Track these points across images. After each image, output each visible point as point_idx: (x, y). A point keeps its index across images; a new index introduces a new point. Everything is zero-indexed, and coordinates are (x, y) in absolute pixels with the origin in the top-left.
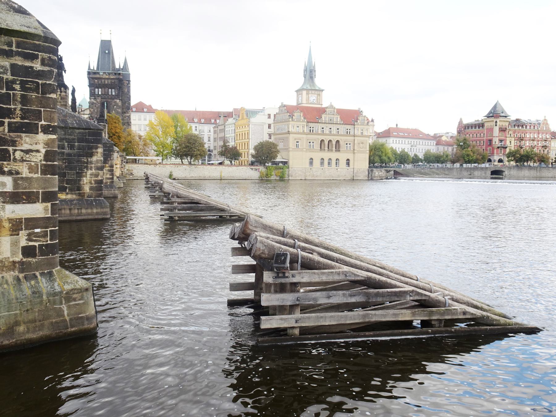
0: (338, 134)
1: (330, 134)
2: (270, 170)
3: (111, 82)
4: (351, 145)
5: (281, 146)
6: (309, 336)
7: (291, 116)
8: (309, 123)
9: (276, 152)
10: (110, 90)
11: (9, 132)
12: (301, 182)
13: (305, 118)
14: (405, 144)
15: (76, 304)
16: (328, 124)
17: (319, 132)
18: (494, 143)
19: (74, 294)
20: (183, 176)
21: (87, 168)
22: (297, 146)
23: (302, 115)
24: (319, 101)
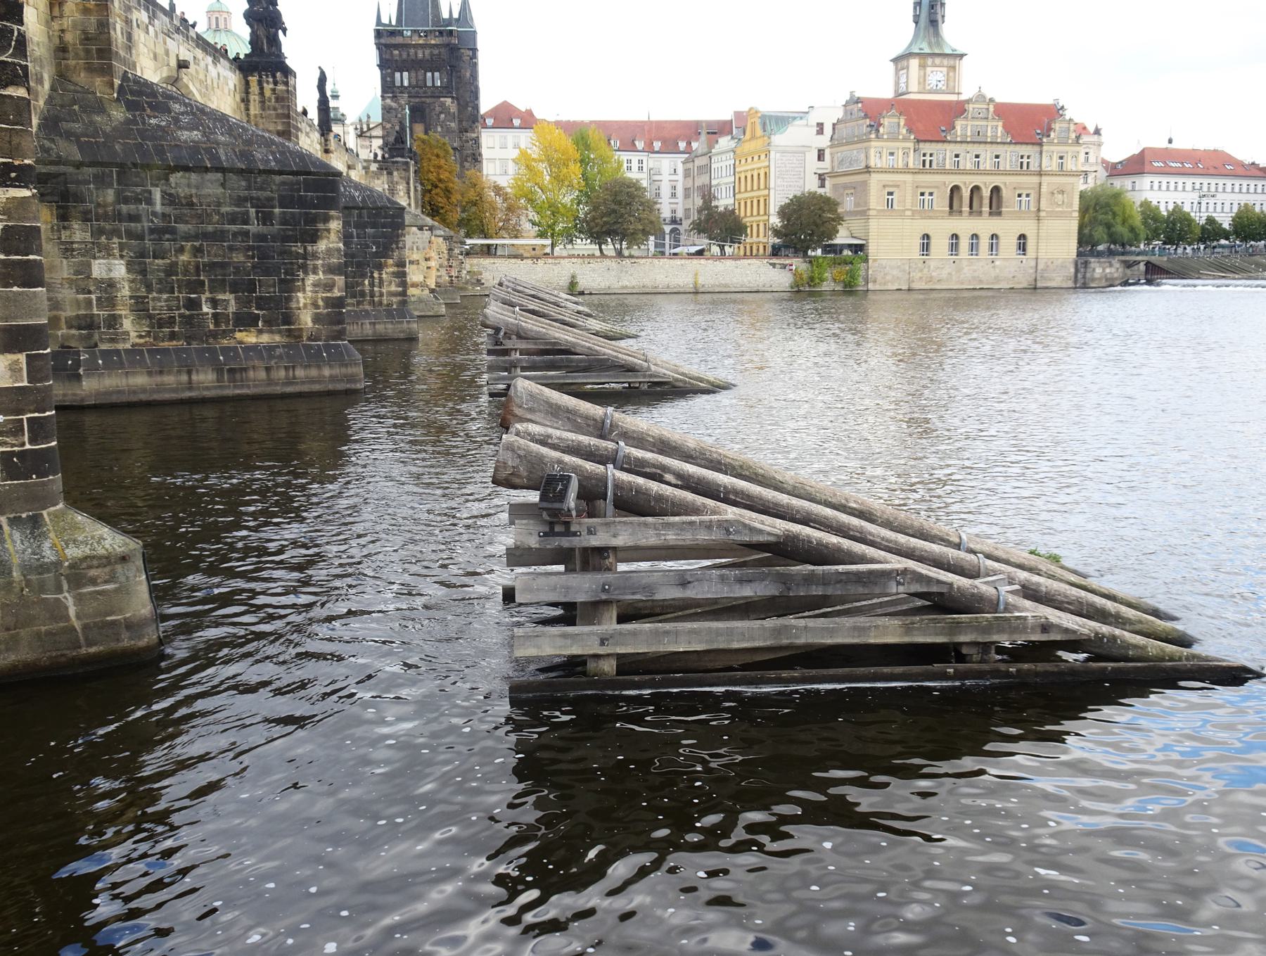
0: (997, 171)
1: (977, 171)
2: (819, 266)
3: (432, 55)
4: (1032, 198)
5: (848, 204)
6: (637, 678)
7: (875, 127)
8: (922, 145)
9: (833, 220)
10: (429, 74)
12: (898, 295)
13: (910, 131)
14: (1184, 190)
15: (98, 593)
16: (970, 145)
17: (947, 167)
19: (90, 567)
20: (603, 285)
21: (304, 268)
22: (890, 204)
23: (902, 123)
24: (951, 84)
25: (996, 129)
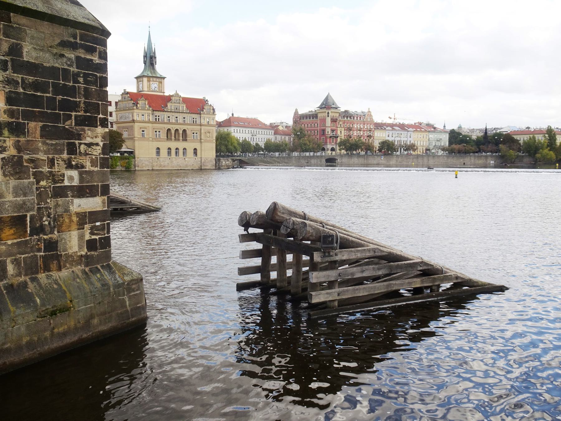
0: (184, 124)
1: (177, 123)
2: (115, 160)
4: (198, 134)
5: (125, 135)
6: (348, 307)
7: (136, 104)
8: (155, 112)
9: (121, 141)
11: (75, 125)
12: (148, 172)
13: (150, 107)
14: (245, 133)
15: (135, 295)
16: (174, 113)
18: (327, 133)
19: (133, 284)
22: (143, 135)
23: (147, 103)
25: (184, 107)
